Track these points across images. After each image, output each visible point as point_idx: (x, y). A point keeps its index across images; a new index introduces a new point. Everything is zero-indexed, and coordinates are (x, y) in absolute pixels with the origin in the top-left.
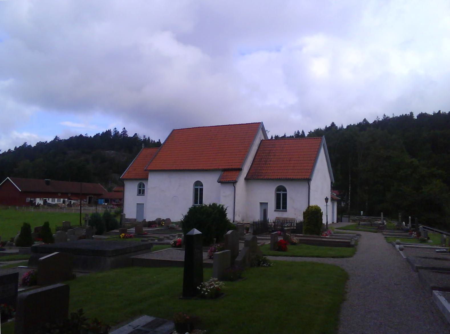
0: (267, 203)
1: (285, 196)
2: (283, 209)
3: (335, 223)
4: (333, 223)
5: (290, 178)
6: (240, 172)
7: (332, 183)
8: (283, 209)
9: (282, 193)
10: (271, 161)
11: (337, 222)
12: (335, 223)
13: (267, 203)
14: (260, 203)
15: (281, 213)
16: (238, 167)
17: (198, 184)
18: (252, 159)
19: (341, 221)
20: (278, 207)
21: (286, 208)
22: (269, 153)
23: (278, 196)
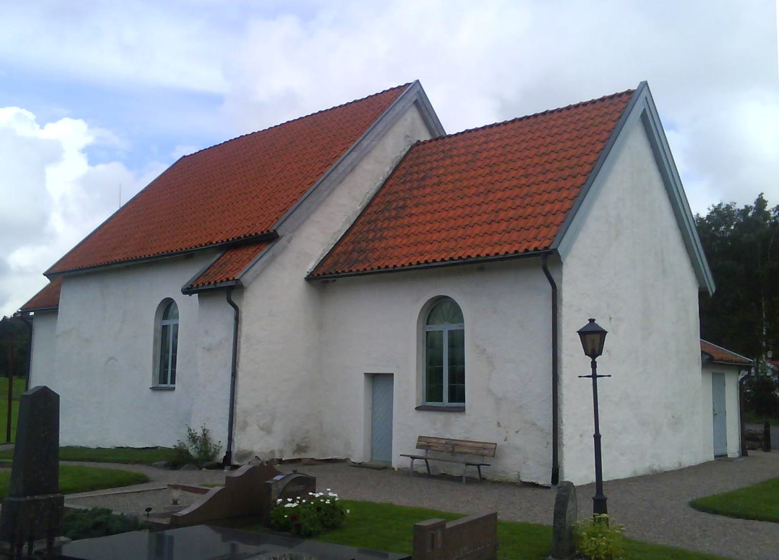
0: (391, 376)
1: (457, 342)
2: (451, 399)
3: (729, 456)
4: (721, 458)
5: (469, 257)
6: (269, 246)
7: (703, 294)
8: (449, 401)
9: (444, 328)
10: (416, 206)
11: (744, 452)
12: (732, 460)
13: (391, 376)
14: (365, 374)
15: (440, 417)
16: (258, 229)
17: (167, 307)
18: (359, 208)
19: (767, 448)
20: (432, 392)
21: (462, 399)
22: (423, 179)
23: (431, 345)
